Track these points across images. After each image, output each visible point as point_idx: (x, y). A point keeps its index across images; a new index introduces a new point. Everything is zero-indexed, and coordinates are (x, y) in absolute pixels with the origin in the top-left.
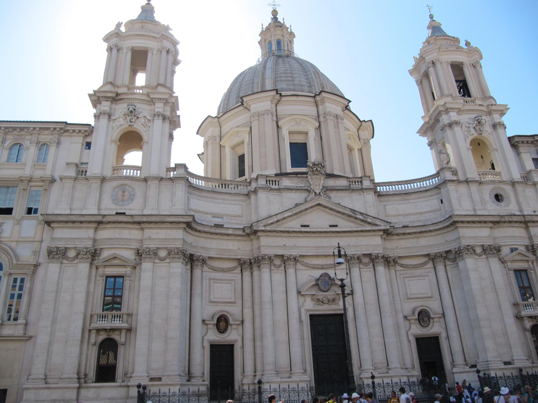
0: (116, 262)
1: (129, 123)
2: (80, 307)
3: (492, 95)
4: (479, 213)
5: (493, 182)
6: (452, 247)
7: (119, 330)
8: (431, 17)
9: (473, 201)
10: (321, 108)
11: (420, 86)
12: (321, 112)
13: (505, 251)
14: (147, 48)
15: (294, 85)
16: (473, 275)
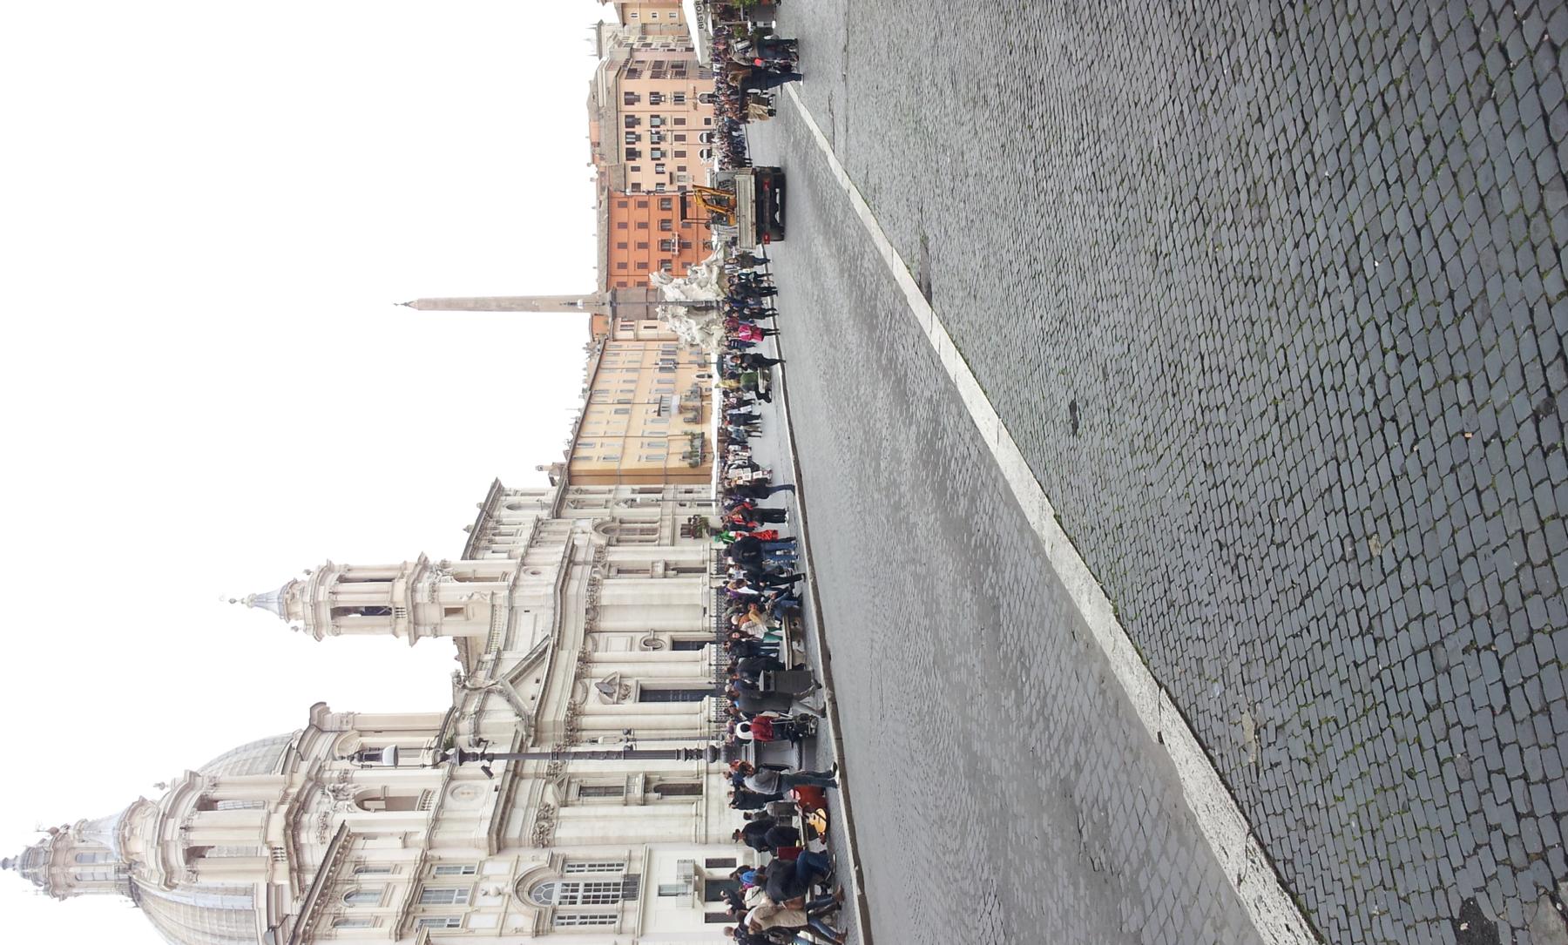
0: (564, 788)
1: (351, 797)
2: (617, 810)
3: (402, 562)
4: (554, 580)
5: (519, 571)
6: (583, 606)
7: (647, 781)
8: (233, 601)
9: (537, 586)
10: (327, 727)
11: (342, 630)
12: (335, 727)
13: (598, 576)
14: (202, 798)
15: (265, 756)
16: (618, 591)
